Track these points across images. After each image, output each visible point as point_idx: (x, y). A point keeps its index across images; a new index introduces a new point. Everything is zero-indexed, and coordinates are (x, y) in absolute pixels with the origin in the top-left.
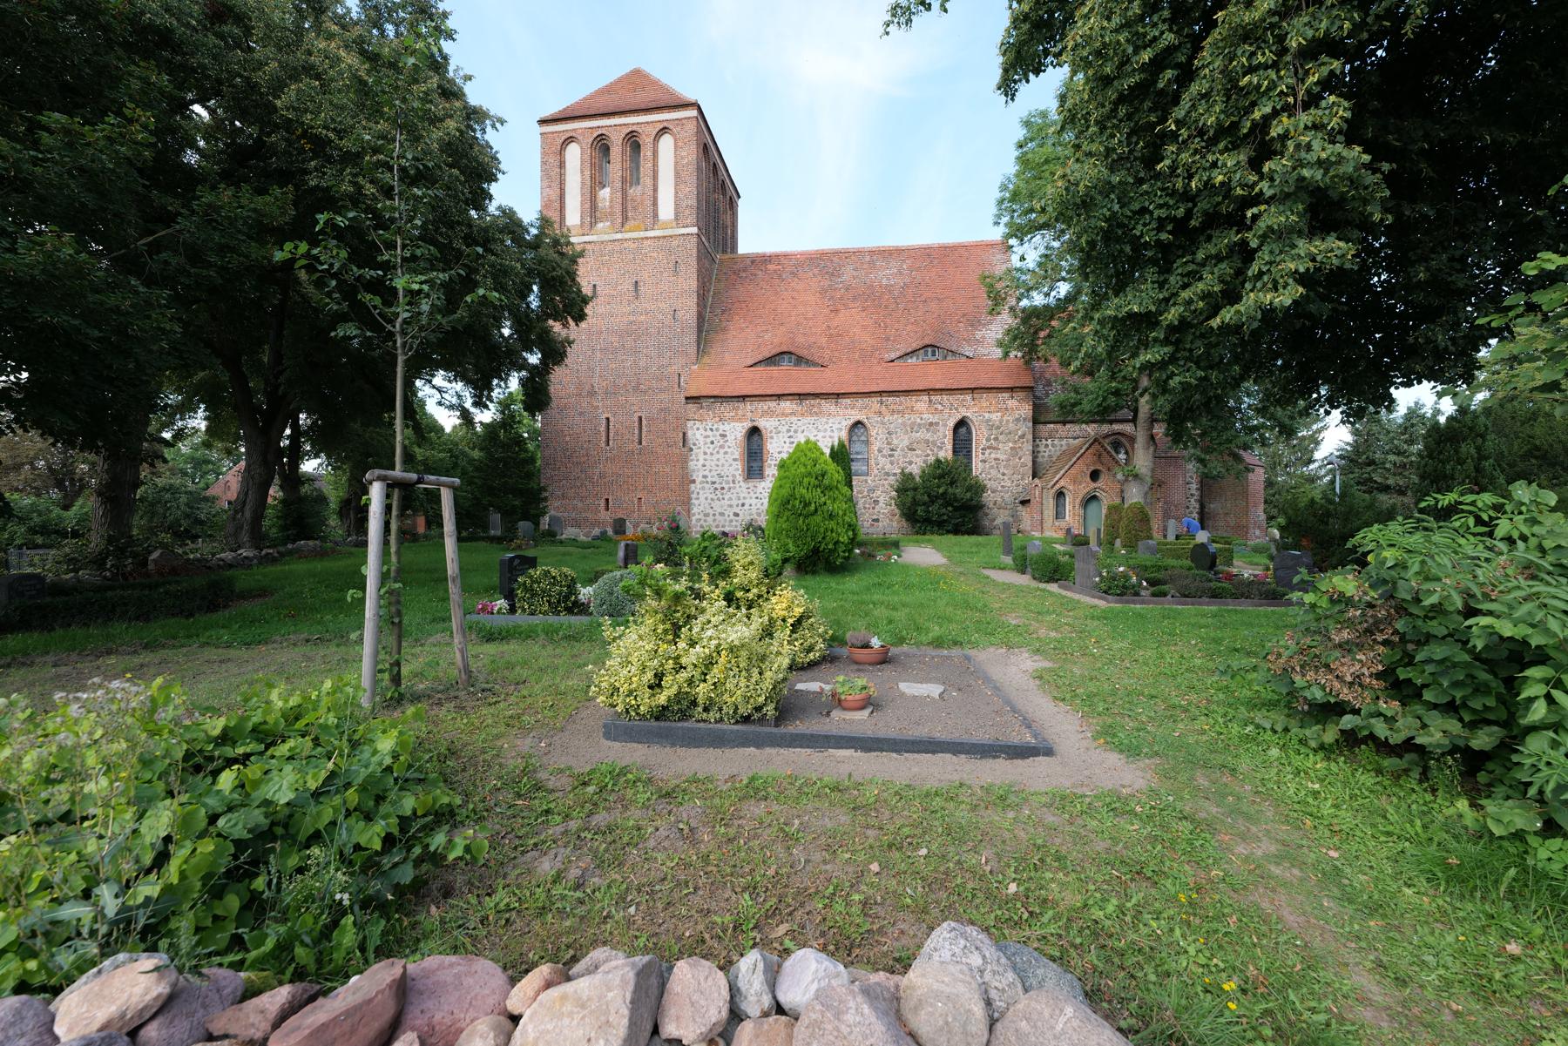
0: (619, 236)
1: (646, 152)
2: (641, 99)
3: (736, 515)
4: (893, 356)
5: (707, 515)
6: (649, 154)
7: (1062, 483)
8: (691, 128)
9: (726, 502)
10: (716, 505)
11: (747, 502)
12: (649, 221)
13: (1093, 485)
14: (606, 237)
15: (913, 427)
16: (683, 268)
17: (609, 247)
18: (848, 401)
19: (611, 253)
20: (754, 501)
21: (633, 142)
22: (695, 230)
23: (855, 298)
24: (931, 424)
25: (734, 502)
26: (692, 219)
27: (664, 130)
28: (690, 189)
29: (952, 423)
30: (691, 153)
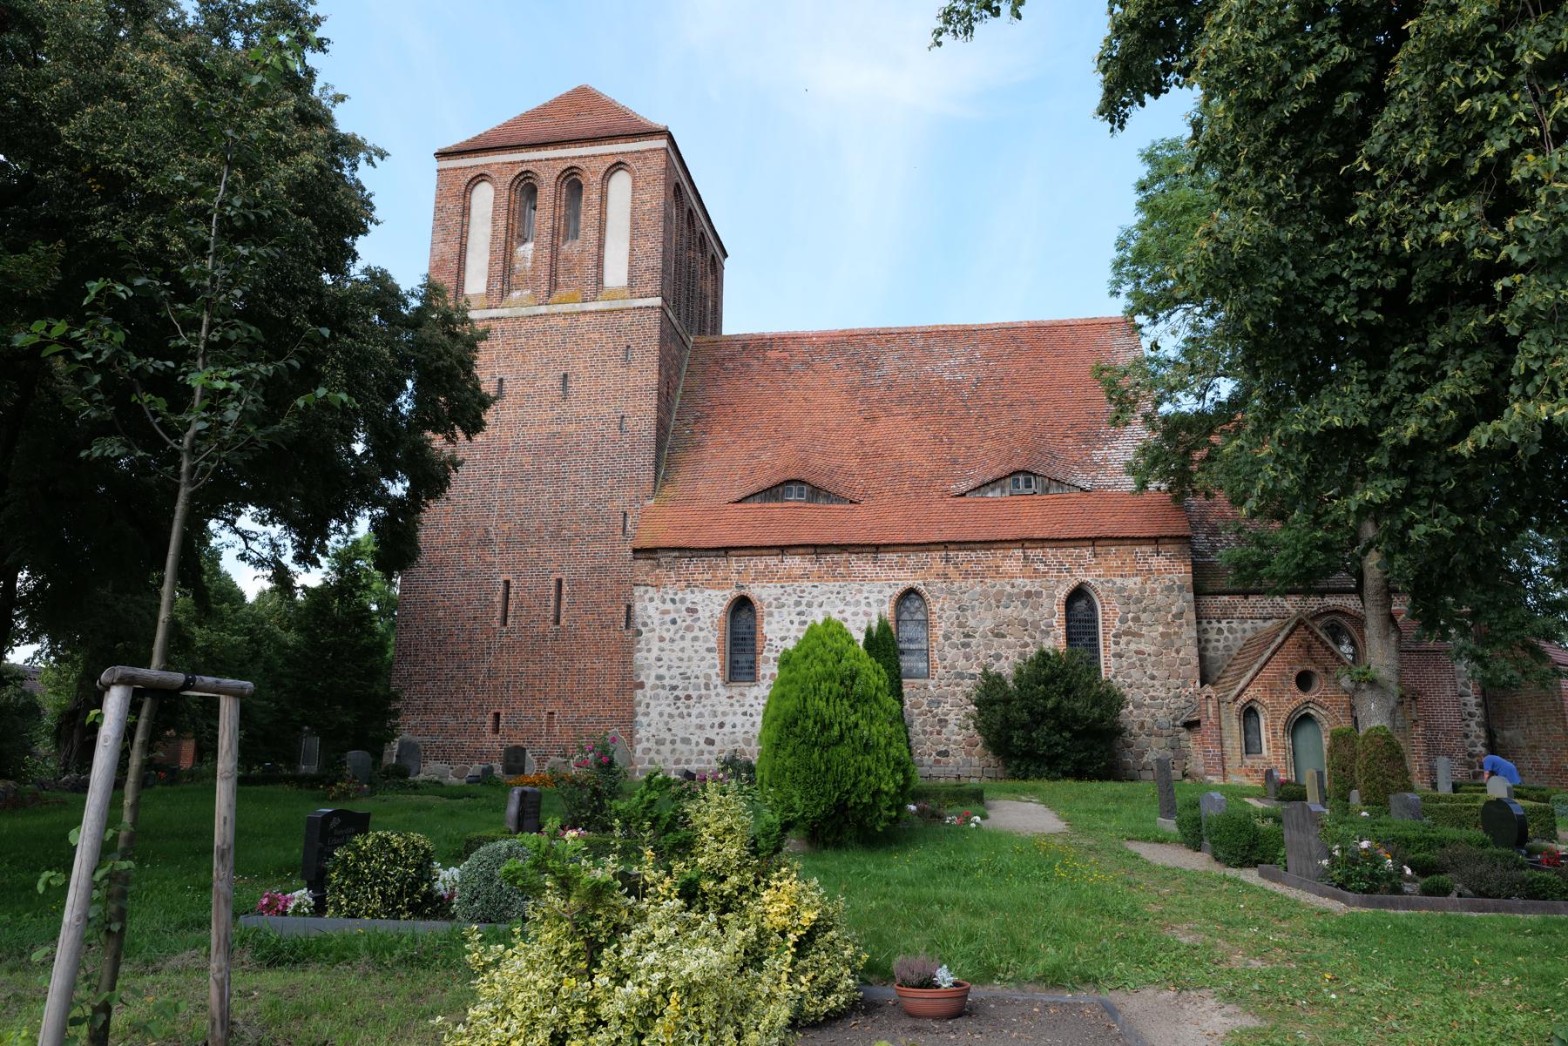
0: (543, 309)
1: (591, 195)
2: (587, 124)
3: (710, 742)
4: (963, 487)
5: (660, 742)
6: (595, 197)
7: (1251, 692)
8: (658, 162)
9: (694, 720)
11: (729, 720)
12: (589, 289)
13: (1303, 697)
14: (524, 311)
15: (1000, 600)
16: (637, 355)
17: (527, 325)
18: (894, 557)
19: (529, 335)
20: (739, 719)
21: (572, 181)
22: (658, 301)
23: (901, 400)
24: (1029, 594)
26: (655, 286)
27: (618, 166)
28: (653, 245)
29: (1062, 593)
30: (656, 196)
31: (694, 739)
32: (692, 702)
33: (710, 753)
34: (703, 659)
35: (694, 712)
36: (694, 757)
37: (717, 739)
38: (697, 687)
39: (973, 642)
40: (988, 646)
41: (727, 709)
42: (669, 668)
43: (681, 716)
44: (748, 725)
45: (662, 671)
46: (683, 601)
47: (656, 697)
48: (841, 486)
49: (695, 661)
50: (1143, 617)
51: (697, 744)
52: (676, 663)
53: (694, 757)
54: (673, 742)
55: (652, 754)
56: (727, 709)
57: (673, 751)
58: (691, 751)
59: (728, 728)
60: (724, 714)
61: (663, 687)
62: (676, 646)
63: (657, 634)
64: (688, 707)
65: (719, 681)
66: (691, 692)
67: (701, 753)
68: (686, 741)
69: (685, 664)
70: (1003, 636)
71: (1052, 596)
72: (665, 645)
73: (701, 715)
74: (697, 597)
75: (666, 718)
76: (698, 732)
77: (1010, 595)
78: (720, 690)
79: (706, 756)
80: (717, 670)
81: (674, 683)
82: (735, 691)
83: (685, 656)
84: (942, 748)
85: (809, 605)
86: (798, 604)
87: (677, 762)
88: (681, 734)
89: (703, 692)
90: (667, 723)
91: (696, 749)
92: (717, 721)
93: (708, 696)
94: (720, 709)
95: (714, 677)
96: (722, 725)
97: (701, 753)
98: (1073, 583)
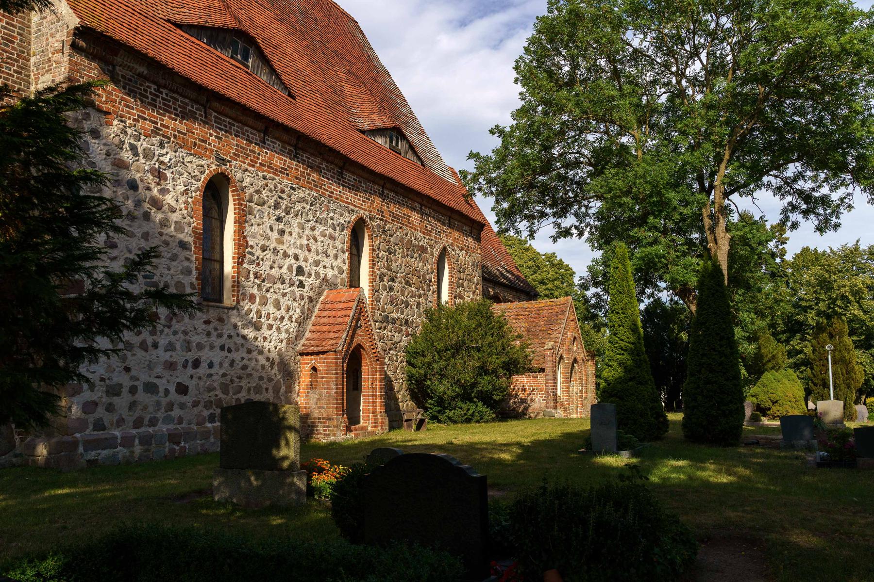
3: (182, 389)
5: (114, 391)
20: (217, 356)
24: (423, 250)
31: (162, 384)
33: (182, 406)
35: (163, 342)
37: (191, 384)
41: (203, 339)
50: (465, 284)
51: (167, 392)
53: (160, 415)
54: (133, 390)
55: (100, 412)
56: (203, 339)
57: (132, 405)
58: (158, 404)
59: (203, 370)
60: (200, 347)
68: (150, 388)
73: (170, 347)
76: (166, 374)
79: (176, 413)
86: (277, 206)
88: (144, 377)
91: (164, 401)
92: (191, 356)
96: (196, 364)
97: (170, 406)
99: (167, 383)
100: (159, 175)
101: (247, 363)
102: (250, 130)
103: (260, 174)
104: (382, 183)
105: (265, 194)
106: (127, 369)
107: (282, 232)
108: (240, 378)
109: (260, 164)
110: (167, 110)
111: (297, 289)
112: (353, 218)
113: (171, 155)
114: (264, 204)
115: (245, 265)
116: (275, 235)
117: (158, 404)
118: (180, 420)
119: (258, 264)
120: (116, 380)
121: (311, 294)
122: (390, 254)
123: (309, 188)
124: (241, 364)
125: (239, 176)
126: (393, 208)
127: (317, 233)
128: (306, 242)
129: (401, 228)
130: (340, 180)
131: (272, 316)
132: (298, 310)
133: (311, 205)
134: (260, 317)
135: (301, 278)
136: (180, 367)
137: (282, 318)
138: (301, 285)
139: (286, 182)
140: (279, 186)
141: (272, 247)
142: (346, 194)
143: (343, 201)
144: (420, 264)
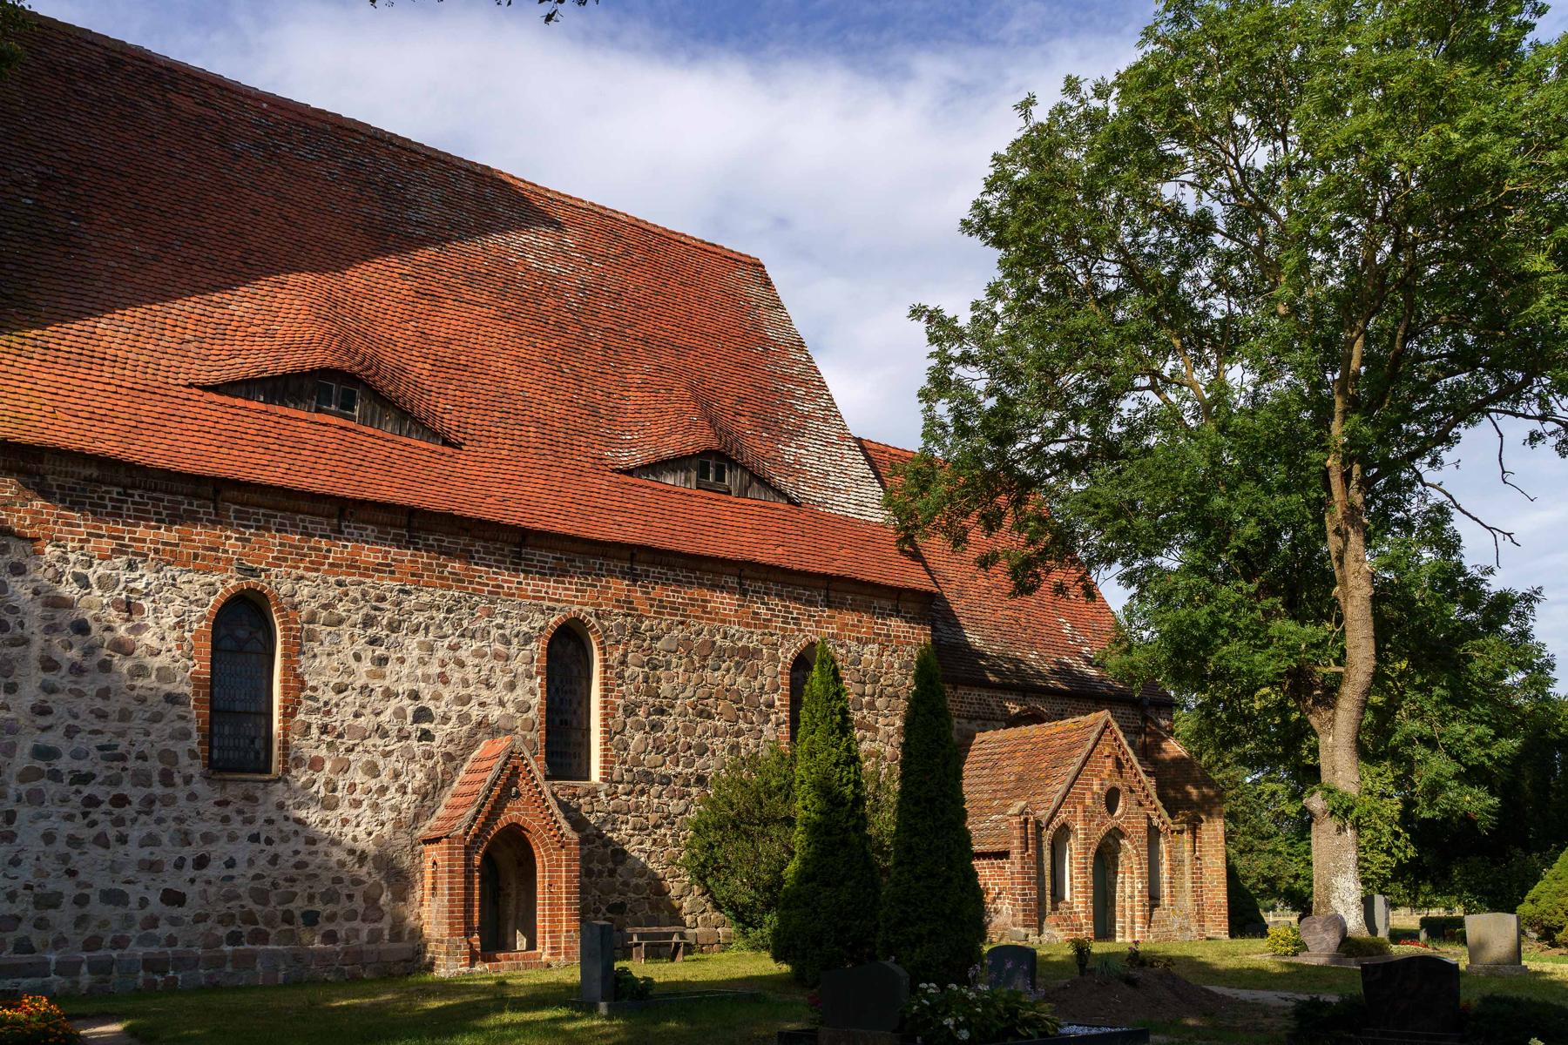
3: (174, 898)
5: (50, 901)
9: (135, 852)
10: (91, 862)
11: (219, 851)
15: (710, 654)
18: (550, 558)
20: (242, 851)
24: (749, 654)
25: (167, 852)
29: (787, 655)
31: (134, 893)
32: (129, 812)
33: (174, 921)
34: (157, 718)
35: (135, 833)
36: (134, 933)
37: (192, 892)
38: (142, 779)
39: (669, 721)
40: (688, 731)
41: (216, 828)
42: (71, 732)
43: (102, 841)
44: (262, 862)
45: (52, 739)
46: (104, 583)
47: (36, 798)
48: (445, 409)
49: (137, 722)
50: (879, 703)
51: (144, 903)
52: (88, 722)
53: (134, 933)
54: (82, 900)
56: (216, 828)
57: (81, 921)
58: (128, 920)
59: (215, 870)
60: (208, 838)
61: (55, 776)
62: (90, 685)
63: (35, 651)
64: (119, 822)
65: (197, 769)
66: (126, 788)
67: (153, 922)
69: (114, 725)
70: (710, 716)
71: (774, 659)
72: (60, 679)
73: (151, 840)
74: (145, 577)
75: (60, 846)
76: (145, 878)
77: (723, 650)
78: (198, 786)
79: (164, 930)
80: (194, 742)
81: (84, 766)
82: (233, 791)
83: (113, 706)
84: (615, 899)
85: (394, 627)
86: (368, 622)
87: (92, 944)
88: (102, 882)
89: (158, 789)
90: (65, 858)
91: (139, 915)
92: (190, 853)
93: (168, 801)
94: (198, 828)
95: (184, 760)
96: (202, 862)
97: (153, 922)
98: (802, 643)
99: (148, 890)
100: (129, 608)
101: (307, 858)
102: (308, 518)
103: (332, 580)
104: (627, 554)
105: (340, 609)
106: (72, 873)
107: (382, 661)
108: (292, 880)
109: (331, 565)
110: (141, 516)
111: (416, 743)
112: (552, 620)
113: (150, 576)
114: (340, 622)
115: (301, 717)
116: (366, 665)
117: (128, 920)
118: (172, 941)
119: (328, 713)
120: (51, 886)
121: (450, 748)
122: (655, 668)
123: (442, 586)
124: (293, 861)
125: (286, 588)
126: (657, 592)
127: (463, 654)
128: (439, 670)
129: (682, 623)
130: (518, 563)
131: (359, 787)
132: (419, 775)
133: (449, 611)
134: (334, 790)
135: (425, 726)
136: (169, 868)
137: (383, 790)
138: (426, 736)
139: (387, 583)
140: (373, 593)
141: (358, 685)
142: (531, 584)
143: (528, 597)
144: (741, 679)
